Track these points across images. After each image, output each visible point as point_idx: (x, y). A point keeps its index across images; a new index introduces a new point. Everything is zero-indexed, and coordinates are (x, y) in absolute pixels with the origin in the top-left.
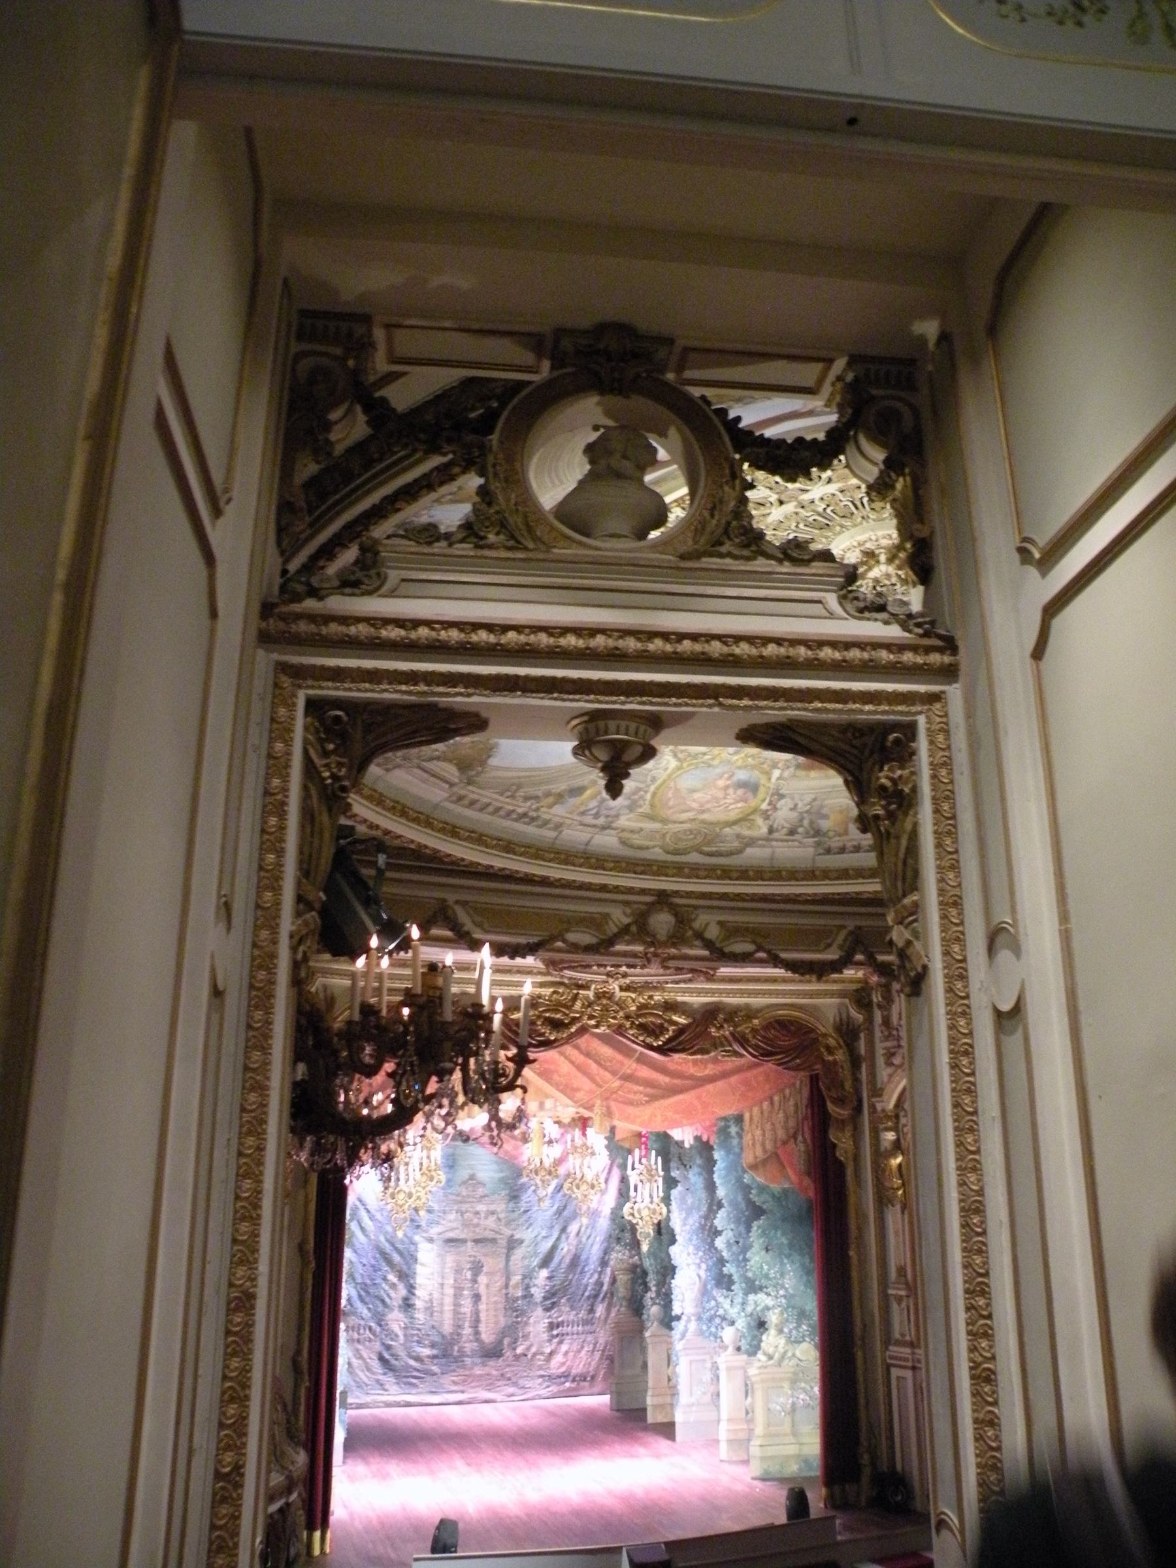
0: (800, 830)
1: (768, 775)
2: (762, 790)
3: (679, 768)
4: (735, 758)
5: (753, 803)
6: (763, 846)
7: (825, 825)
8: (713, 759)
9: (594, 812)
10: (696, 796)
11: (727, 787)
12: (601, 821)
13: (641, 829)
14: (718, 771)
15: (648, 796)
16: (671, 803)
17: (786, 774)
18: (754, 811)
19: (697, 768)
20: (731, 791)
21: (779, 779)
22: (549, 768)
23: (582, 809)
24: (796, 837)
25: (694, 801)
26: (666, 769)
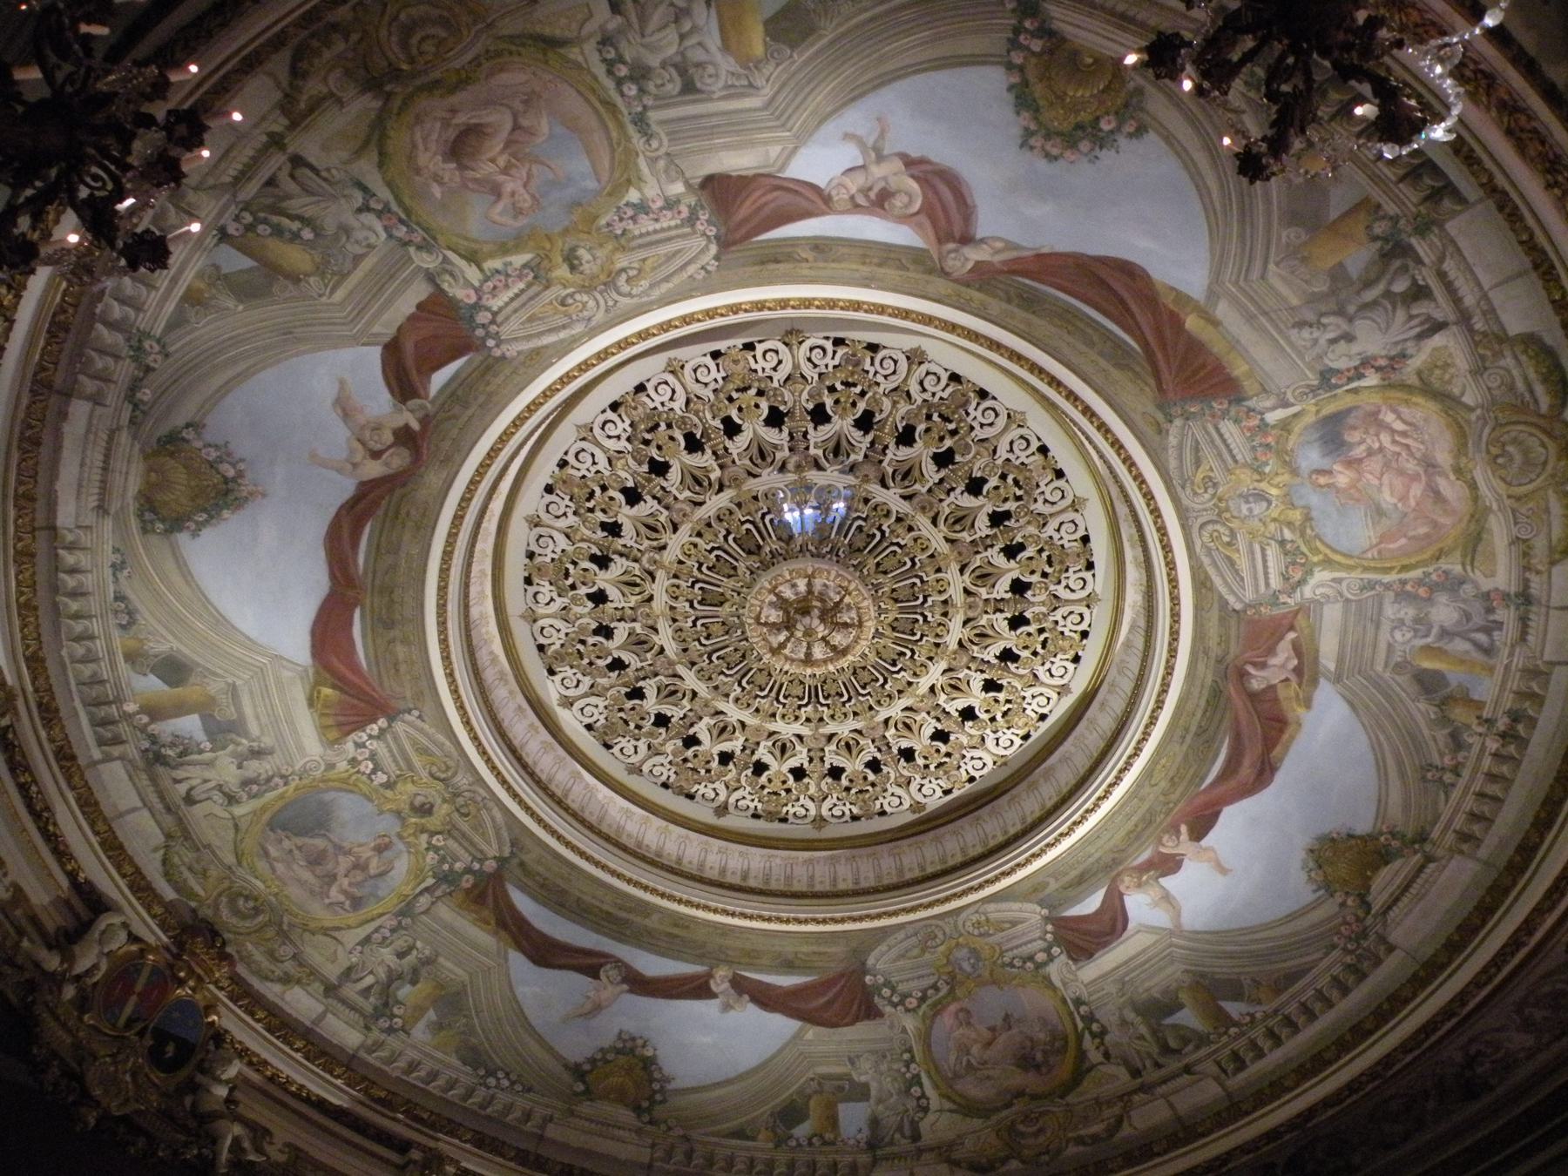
0: (1400, 286)
1: (1285, 426)
2: (1329, 409)
3: (1328, 563)
4: (1274, 491)
5: (1371, 400)
6: (1491, 312)
7: (1358, 257)
8: (1290, 524)
9: (1482, 638)
10: (1387, 498)
11: (1351, 463)
12: (1506, 616)
13: (1516, 541)
14: (1314, 499)
15: (1417, 573)
16: (1423, 530)
17: (1268, 404)
18: (1388, 386)
19: (1317, 537)
20: (1359, 451)
21: (1286, 405)
22: (1376, 747)
23: (1477, 656)
24: (1427, 277)
25: (1404, 498)
26: (1339, 581)
